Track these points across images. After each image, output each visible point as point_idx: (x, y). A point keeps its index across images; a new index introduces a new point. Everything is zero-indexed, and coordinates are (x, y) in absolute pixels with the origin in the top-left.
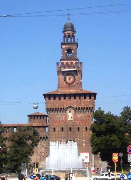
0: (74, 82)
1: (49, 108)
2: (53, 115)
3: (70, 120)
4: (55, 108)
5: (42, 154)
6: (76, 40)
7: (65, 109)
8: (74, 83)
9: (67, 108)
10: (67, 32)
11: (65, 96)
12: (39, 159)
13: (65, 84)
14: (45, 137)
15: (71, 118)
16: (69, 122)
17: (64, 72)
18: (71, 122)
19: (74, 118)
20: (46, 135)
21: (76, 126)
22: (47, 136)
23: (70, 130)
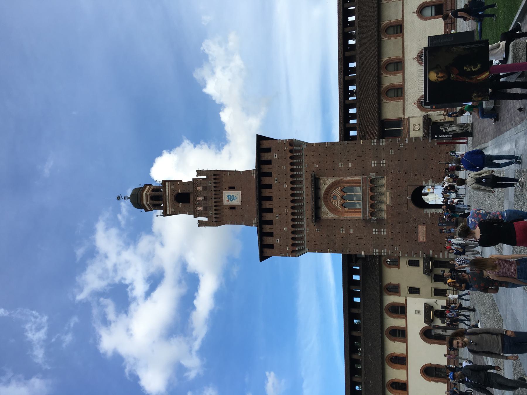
4: (293, 236)
10: (145, 202)
11: (262, 211)
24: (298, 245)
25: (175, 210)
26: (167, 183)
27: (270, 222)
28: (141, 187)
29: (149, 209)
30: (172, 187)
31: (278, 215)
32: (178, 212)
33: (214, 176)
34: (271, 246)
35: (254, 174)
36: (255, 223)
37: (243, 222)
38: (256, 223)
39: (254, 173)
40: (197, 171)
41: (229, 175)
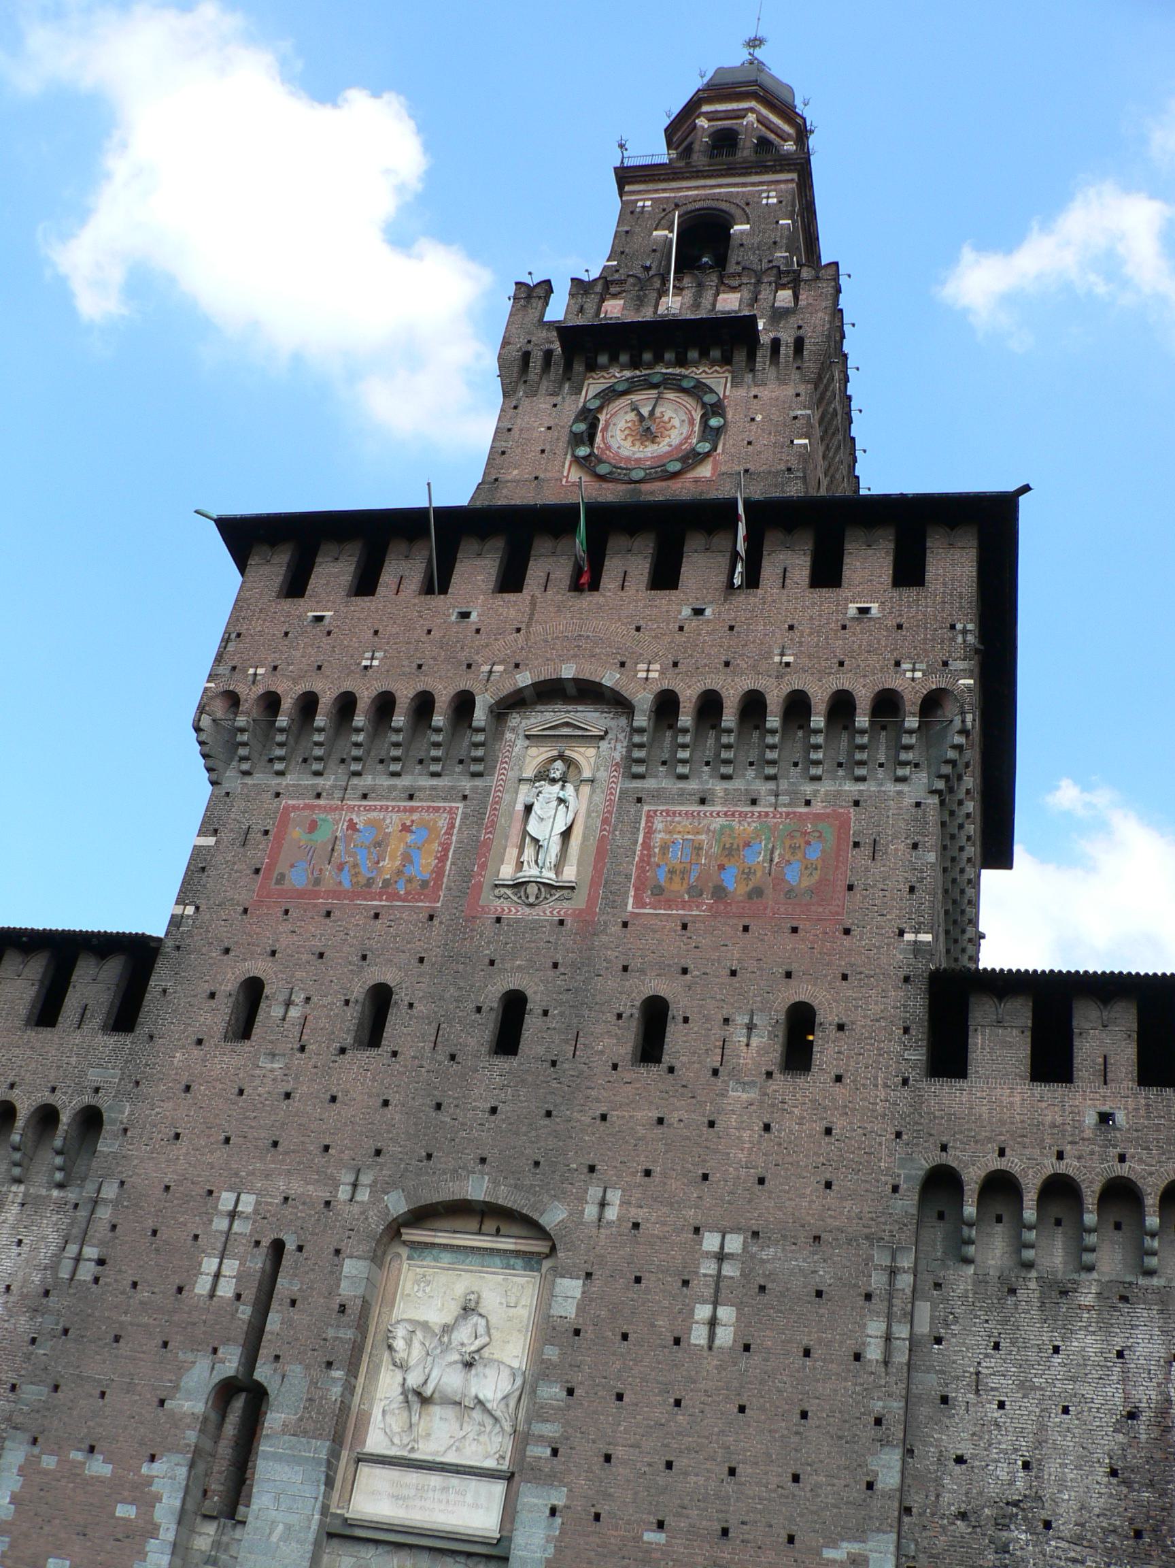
0: (692, 459)
1: (250, 694)
2: (284, 802)
3: (530, 871)
7: (480, 716)
8: (705, 471)
10: (706, 108)
13: (575, 475)
15: (554, 848)
16: (513, 910)
17: (592, 367)
18: (550, 910)
19: (602, 853)
20: (94, 1076)
21: (611, 982)
22: (103, 1102)
25: (642, 212)
26: (794, 176)
30: (768, 197)
31: (474, 617)
33: (791, 340)
41: (792, 414)
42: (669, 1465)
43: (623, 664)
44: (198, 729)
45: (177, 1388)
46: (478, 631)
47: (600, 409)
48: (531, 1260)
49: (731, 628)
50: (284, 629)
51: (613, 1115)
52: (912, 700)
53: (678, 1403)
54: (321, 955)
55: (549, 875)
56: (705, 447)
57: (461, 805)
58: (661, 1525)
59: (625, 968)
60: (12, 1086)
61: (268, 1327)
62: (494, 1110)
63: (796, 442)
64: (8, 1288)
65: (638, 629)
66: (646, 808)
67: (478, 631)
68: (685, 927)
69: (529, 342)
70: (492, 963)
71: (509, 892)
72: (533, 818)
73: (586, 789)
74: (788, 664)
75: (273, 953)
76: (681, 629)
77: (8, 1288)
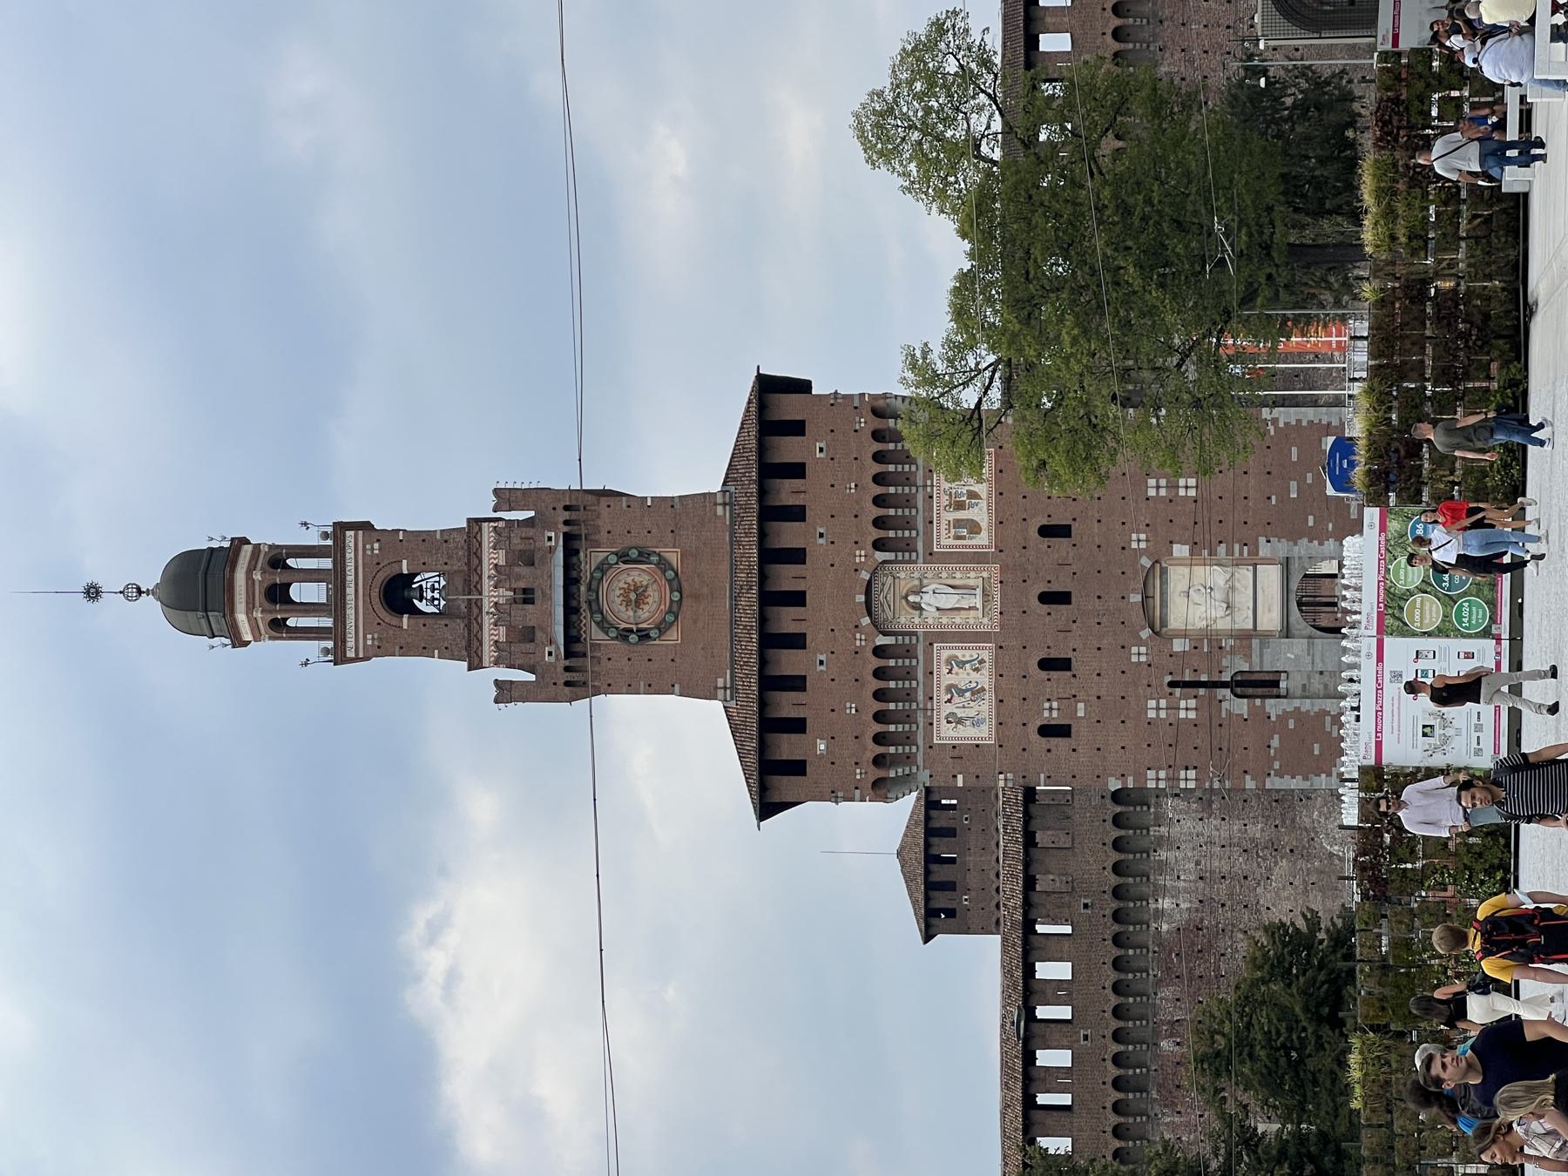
0: (663, 565)
3: (977, 601)
5: (1252, 840)
6: (312, 539)
8: (673, 557)
9: (874, 623)
11: (771, 641)
12: (1301, 864)
13: (673, 636)
14: (1119, 809)
17: (577, 640)
23: (1063, 598)
24: (895, 761)
25: (380, 639)
27: (797, 683)
28: (212, 550)
29: (247, 637)
30: (373, 549)
31: (823, 657)
32: (397, 648)
33: (567, 513)
34: (797, 768)
35: (728, 507)
36: (725, 688)
37: (677, 686)
38: (728, 686)
39: (724, 504)
40: (496, 492)
42: (1246, 498)
43: (856, 570)
44: (897, 799)
45: (1237, 715)
46: (832, 653)
47: (617, 628)
48: (1164, 572)
49: (832, 516)
50: (829, 765)
51: (1097, 541)
52: (878, 423)
53: (1221, 498)
54: (1024, 699)
55: (979, 591)
56: (654, 559)
57: (935, 645)
58: (1269, 498)
59: (1024, 548)
60: (1104, 844)
61: (1206, 679)
62: (1099, 597)
63: (649, 504)
64: (1201, 819)
65: (832, 565)
66: (935, 550)
67: (832, 653)
68: (1001, 523)
69: (555, 684)
70: (1024, 612)
71: (986, 610)
72: (942, 607)
73: (925, 581)
74: (856, 485)
75: (1024, 724)
76: (832, 543)
77: (1201, 819)
